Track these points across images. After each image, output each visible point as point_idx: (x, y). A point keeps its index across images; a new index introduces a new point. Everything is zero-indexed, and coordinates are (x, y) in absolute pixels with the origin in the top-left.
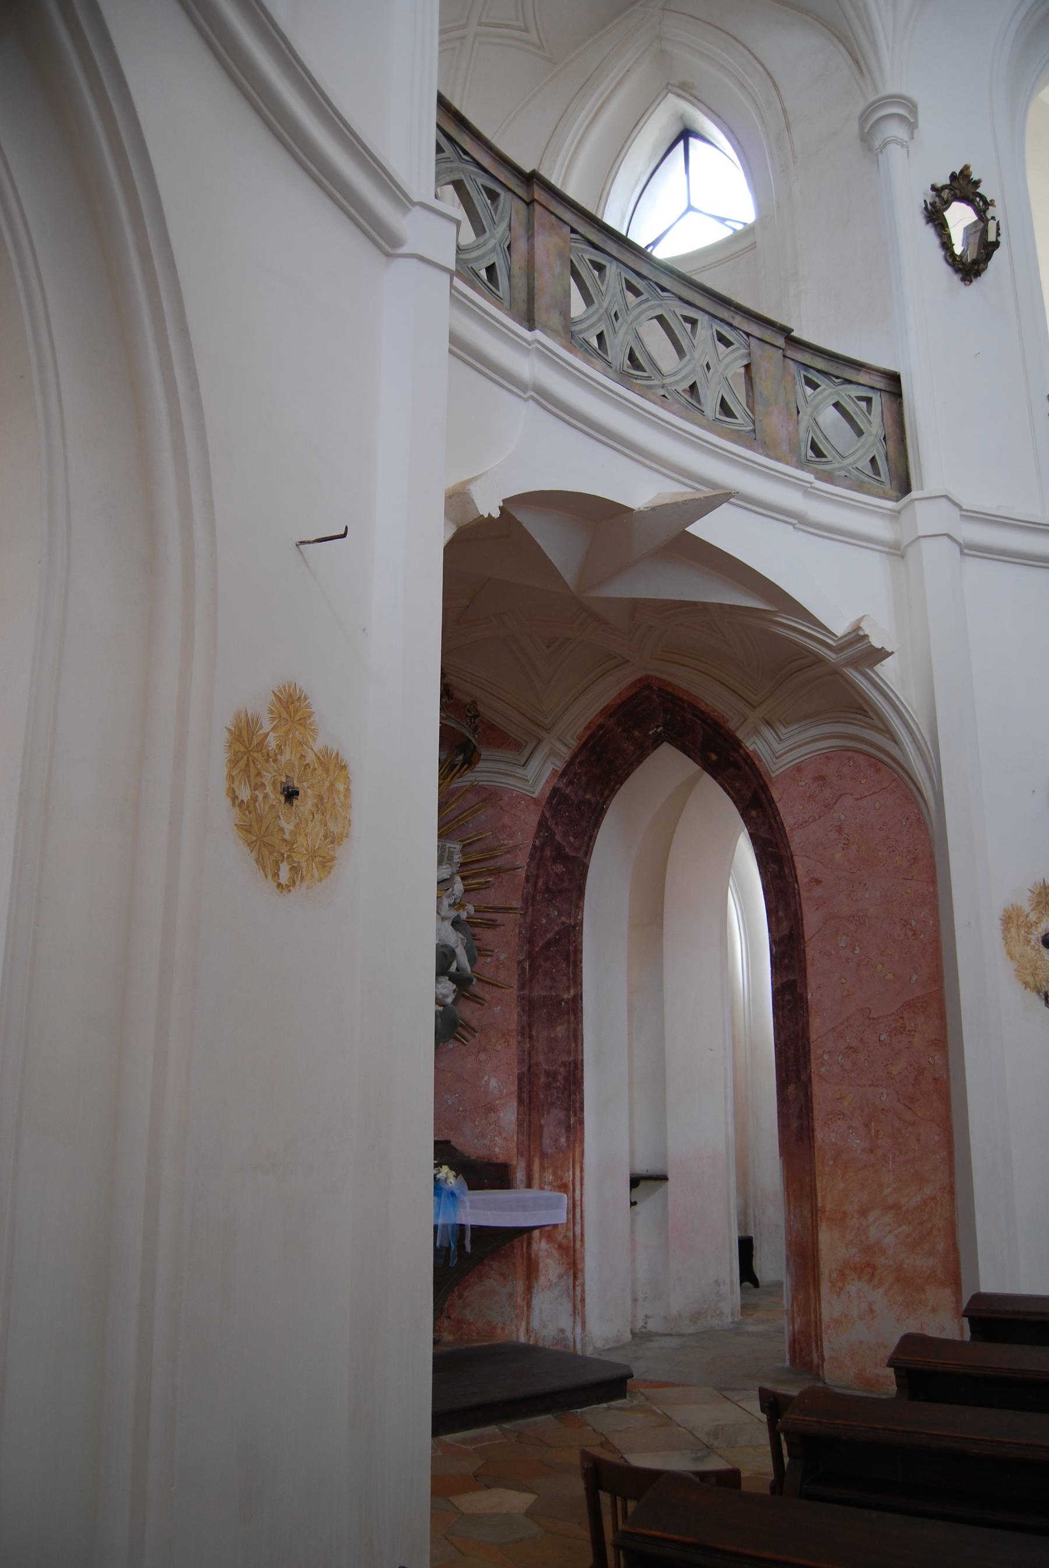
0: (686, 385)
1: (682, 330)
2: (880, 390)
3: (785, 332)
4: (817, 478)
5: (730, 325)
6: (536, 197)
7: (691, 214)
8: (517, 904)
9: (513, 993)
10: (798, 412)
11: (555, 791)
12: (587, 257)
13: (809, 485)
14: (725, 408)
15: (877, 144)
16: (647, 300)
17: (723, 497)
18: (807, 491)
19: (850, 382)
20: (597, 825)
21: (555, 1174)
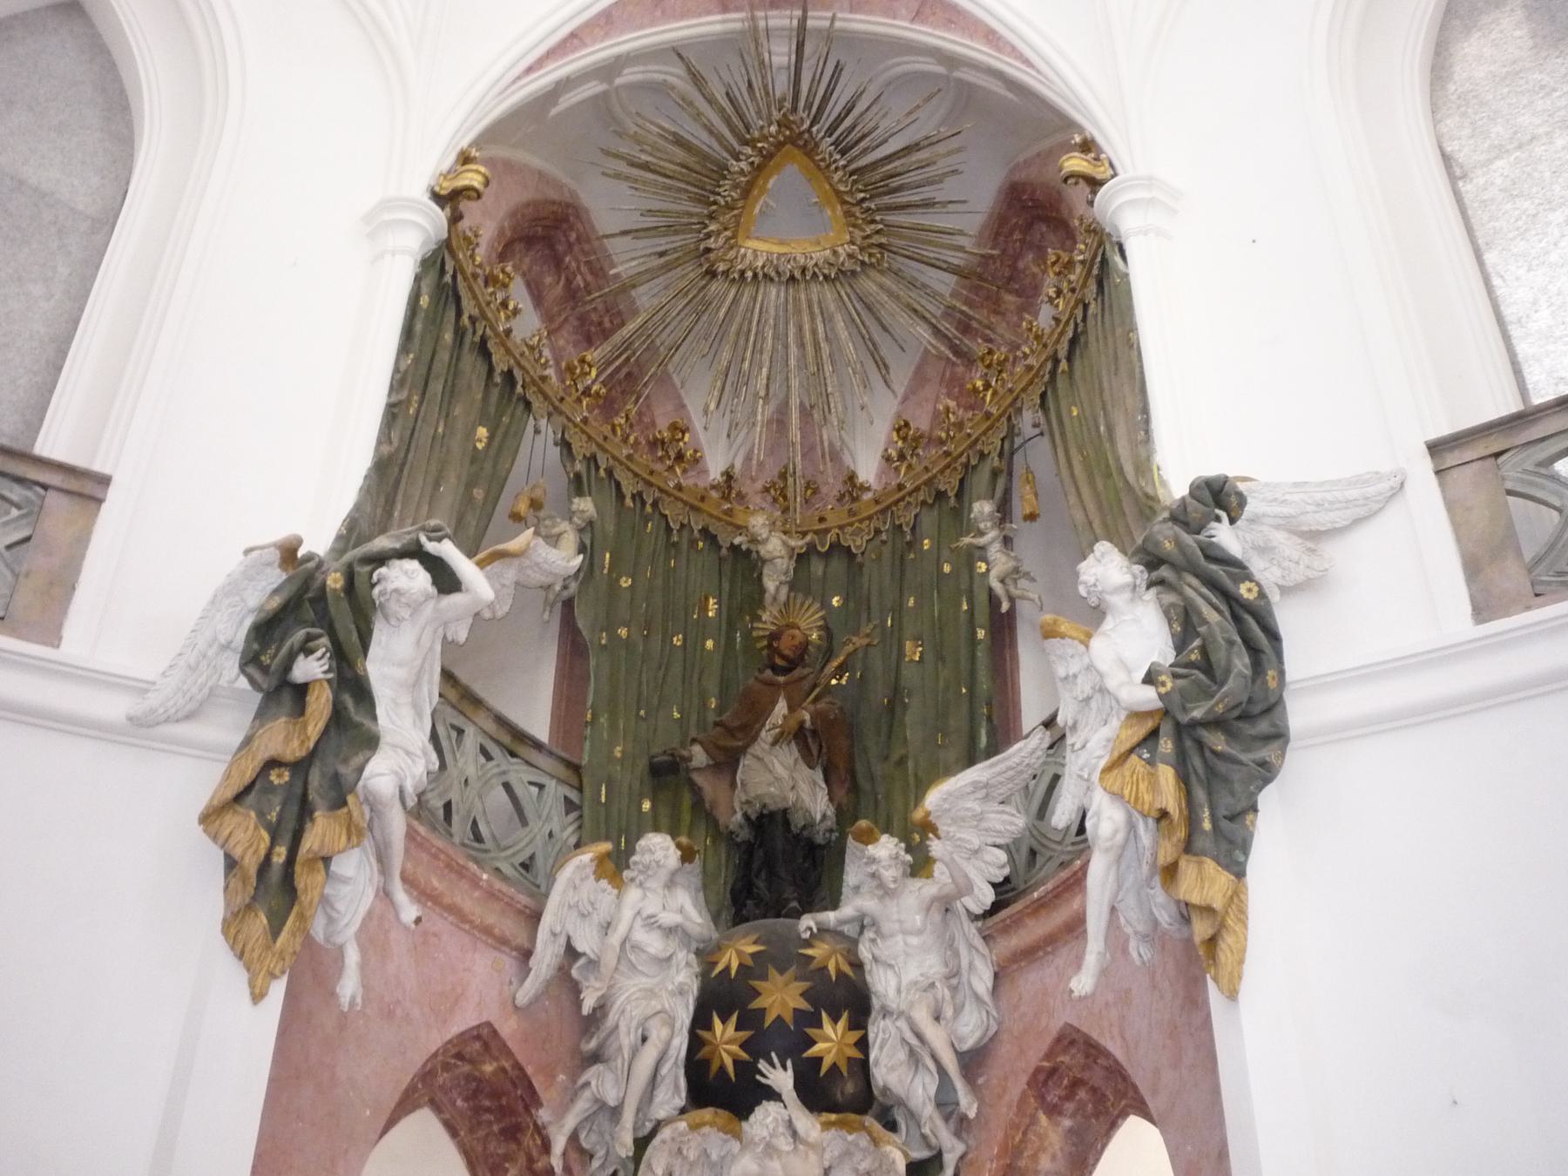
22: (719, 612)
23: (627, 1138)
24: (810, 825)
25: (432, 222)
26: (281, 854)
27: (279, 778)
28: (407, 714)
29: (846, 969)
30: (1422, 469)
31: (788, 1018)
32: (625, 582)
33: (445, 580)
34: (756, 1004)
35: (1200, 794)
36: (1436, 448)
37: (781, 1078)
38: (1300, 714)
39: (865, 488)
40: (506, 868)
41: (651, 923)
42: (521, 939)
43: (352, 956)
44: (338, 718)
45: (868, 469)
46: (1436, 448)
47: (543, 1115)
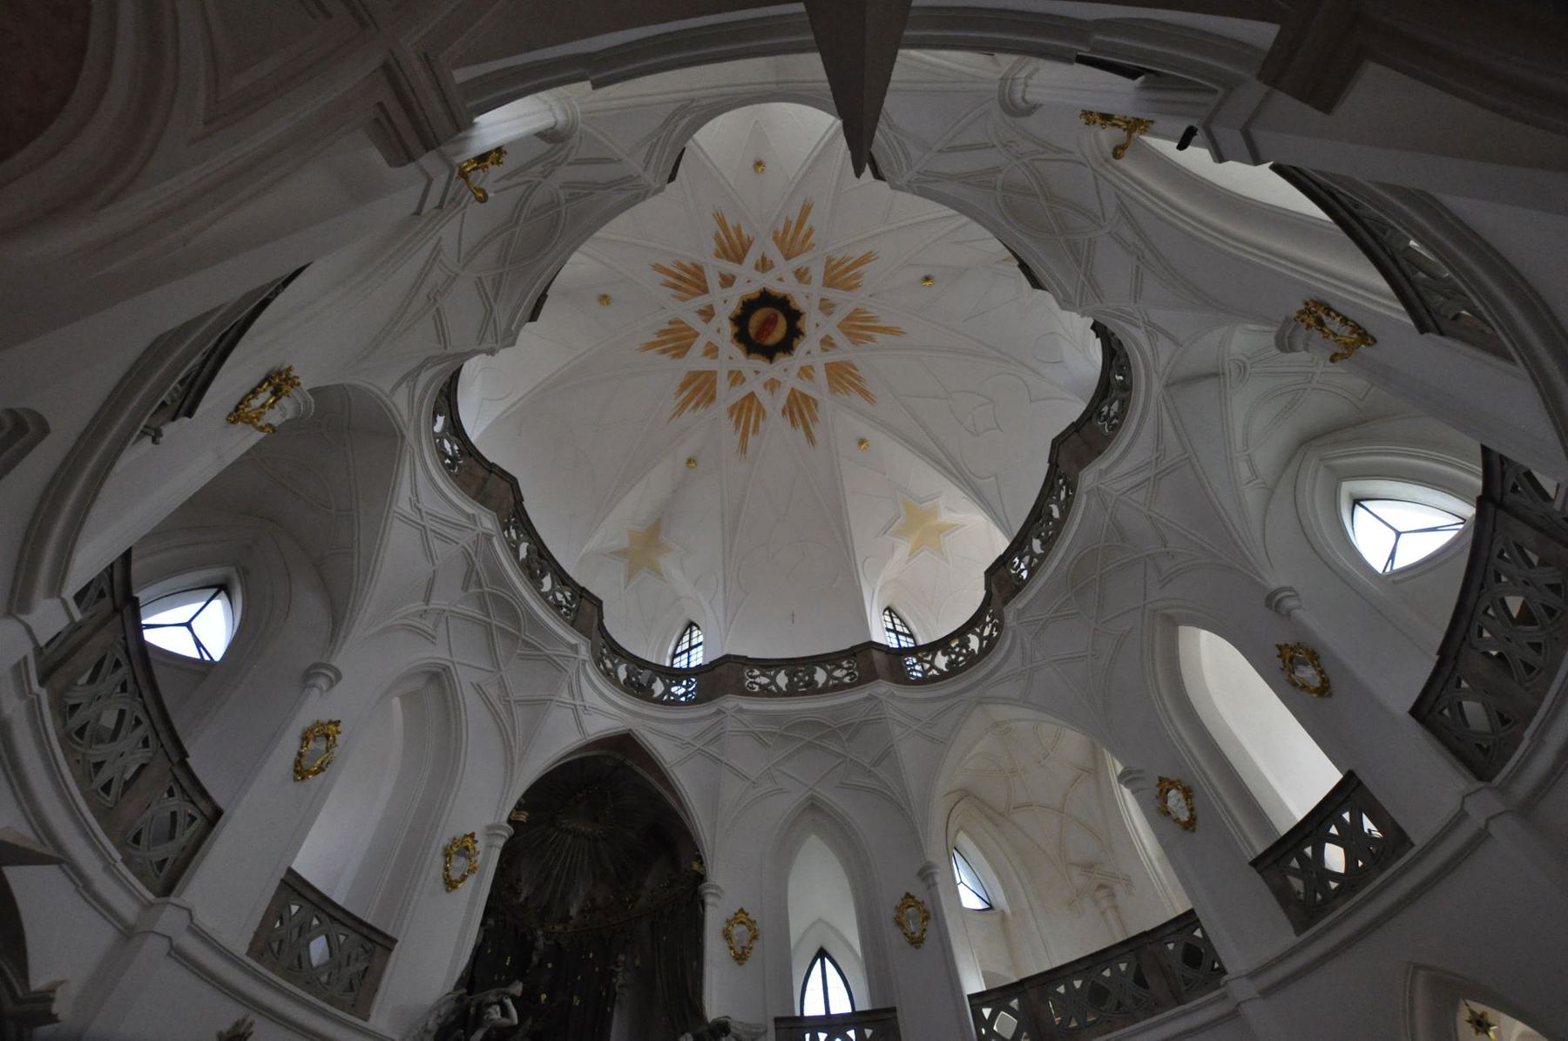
0: (99, 759)
1: (128, 721)
2: (205, 816)
3: (183, 754)
4: (123, 860)
5: (157, 735)
6: (124, 611)
7: (185, 628)
10: (148, 808)
12: (118, 656)
13: (112, 862)
14: (106, 788)
15: (311, 682)
16: (126, 697)
17: (58, 858)
18: (109, 867)
19: (192, 802)
22: (510, 963)
25: (507, 831)
30: (771, 1026)
33: (505, 1012)
39: (571, 918)
45: (573, 911)
46: (777, 1020)
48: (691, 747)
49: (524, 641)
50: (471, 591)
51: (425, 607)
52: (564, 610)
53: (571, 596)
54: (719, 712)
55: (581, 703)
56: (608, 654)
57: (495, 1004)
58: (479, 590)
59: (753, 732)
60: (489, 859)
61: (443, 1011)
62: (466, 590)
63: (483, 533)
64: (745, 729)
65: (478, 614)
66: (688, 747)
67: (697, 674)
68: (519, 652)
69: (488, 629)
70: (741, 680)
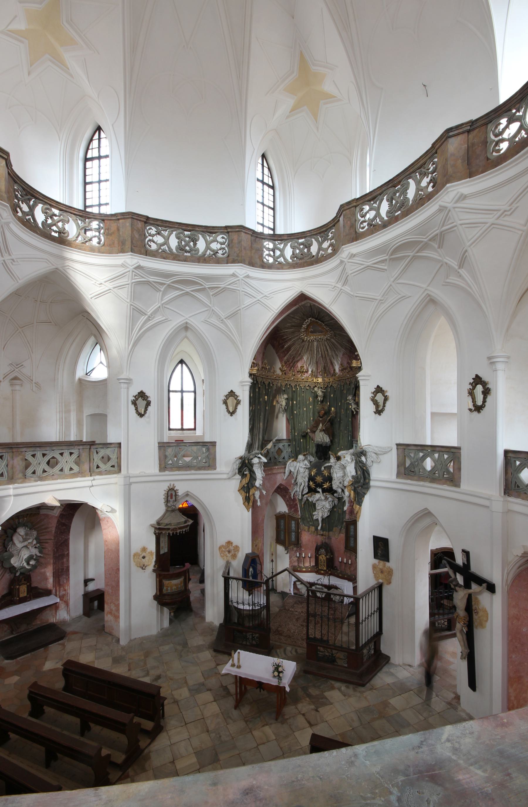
8: (53, 538)
9: (52, 556)
11: (61, 514)
20: (73, 518)
21: (63, 588)
23: (300, 496)
24: (327, 443)
26: (247, 495)
27: (246, 485)
28: (259, 470)
29: (328, 474)
30: (395, 447)
31: (320, 482)
32: (295, 402)
34: (316, 481)
35: (356, 496)
36: (397, 445)
37: (320, 490)
38: (372, 483)
40: (281, 460)
41: (301, 467)
42: (284, 471)
43: (259, 500)
44: (251, 476)
46: (397, 445)
47: (290, 491)
48: (338, 289)
49: (209, 288)
50: (162, 289)
51: (147, 316)
52: (220, 252)
53: (223, 238)
54: (342, 262)
55: (262, 296)
56: (275, 245)
57: (254, 457)
58: (166, 285)
59: (368, 266)
60: (244, 395)
61: (238, 463)
62: (160, 291)
63: (135, 268)
64: (363, 267)
65: (177, 293)
66: (336, 289)
67: (334, 226)
68: (211, 294)
69: (187, 293)
70: (353, 226)
